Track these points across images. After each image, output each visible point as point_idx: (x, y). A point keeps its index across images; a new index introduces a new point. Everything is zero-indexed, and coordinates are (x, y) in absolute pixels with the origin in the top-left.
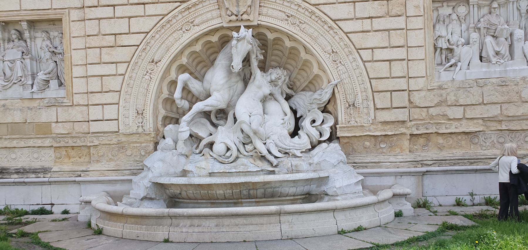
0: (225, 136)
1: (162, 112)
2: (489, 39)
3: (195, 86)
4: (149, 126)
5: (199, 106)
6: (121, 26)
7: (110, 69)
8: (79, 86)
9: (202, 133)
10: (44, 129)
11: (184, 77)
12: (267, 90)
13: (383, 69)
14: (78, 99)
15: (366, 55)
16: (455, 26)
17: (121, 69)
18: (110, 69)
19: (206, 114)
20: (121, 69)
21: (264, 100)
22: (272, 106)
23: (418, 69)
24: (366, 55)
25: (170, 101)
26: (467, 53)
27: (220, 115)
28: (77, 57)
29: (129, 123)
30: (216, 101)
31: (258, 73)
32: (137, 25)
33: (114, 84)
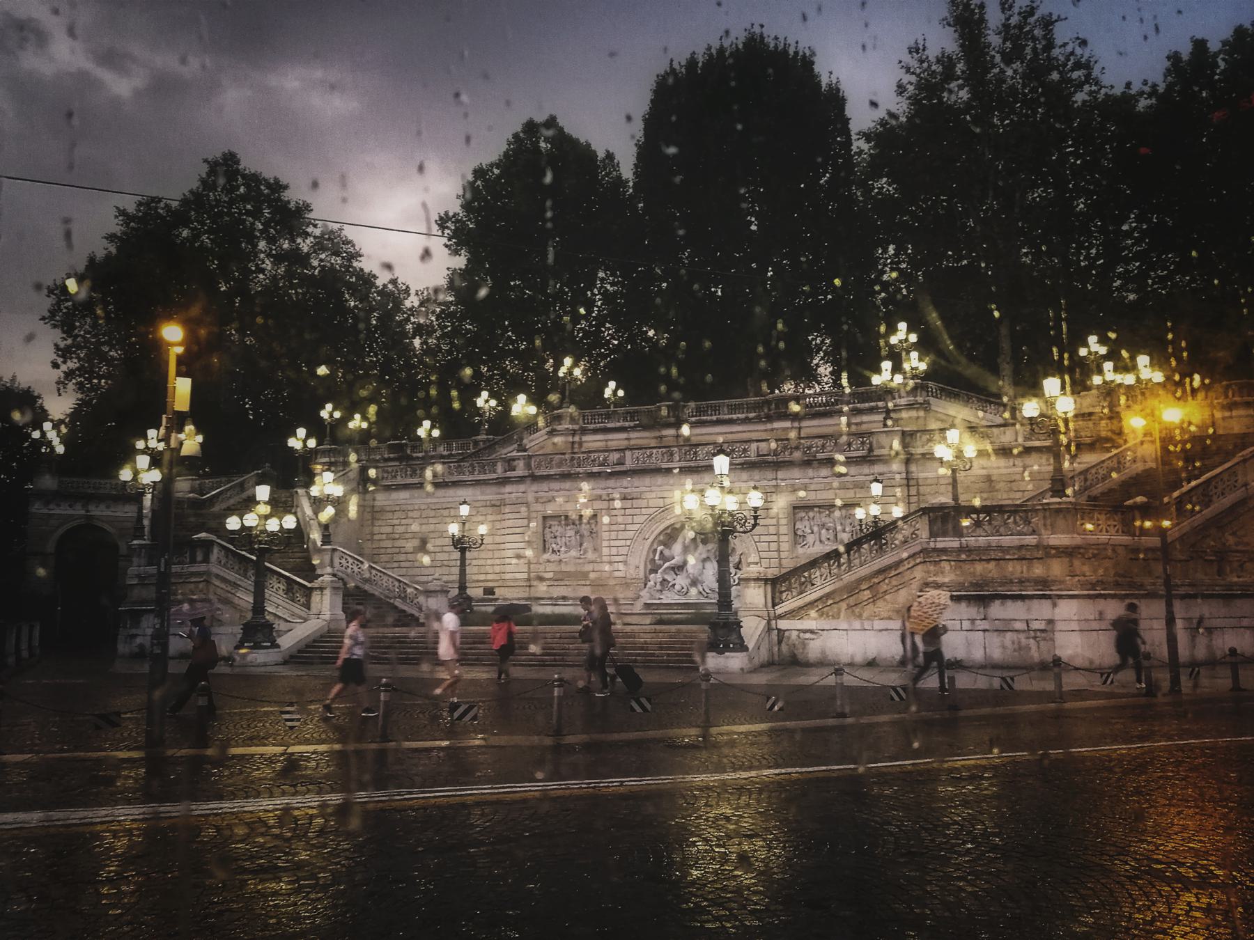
0: (681, 581)
1: (649, 567)
2: (824, 531)
3: (667, 552)
4: (642, 575)
5: (667, 564)
6: (629, 519)
7: (622, 543)
8: (605, 551)
9: (668, 578)
10: (585, 575)
11: (660, 548)
12: (704, 556)
13: (763, 546)
14: (605, 559)
15: (756, 538)
16: (807, 523)
17: (628, 543)
18: (622, 543)
19: (673, 568)
20: (628, 543)
21: (704, 560)
22: (708, 565)
23: (785, 546)
24: (756, 538)
25: (653, 560)
26: (810, 539)
27: (679, 568)
28: (605, 535)
29: (632, 572)
30: (677, 560)
31: (701, 546)
32: (637, 519)
33: (624, 551)
